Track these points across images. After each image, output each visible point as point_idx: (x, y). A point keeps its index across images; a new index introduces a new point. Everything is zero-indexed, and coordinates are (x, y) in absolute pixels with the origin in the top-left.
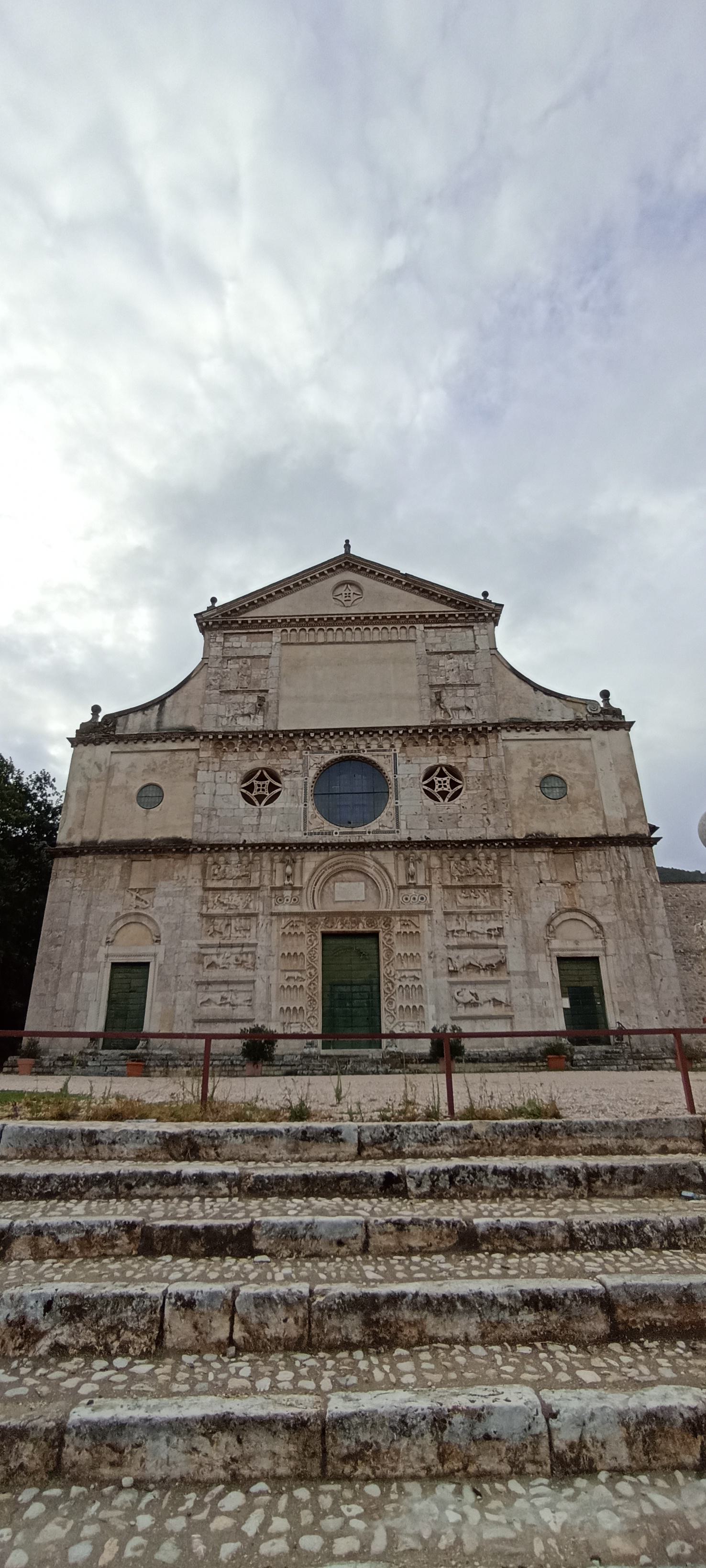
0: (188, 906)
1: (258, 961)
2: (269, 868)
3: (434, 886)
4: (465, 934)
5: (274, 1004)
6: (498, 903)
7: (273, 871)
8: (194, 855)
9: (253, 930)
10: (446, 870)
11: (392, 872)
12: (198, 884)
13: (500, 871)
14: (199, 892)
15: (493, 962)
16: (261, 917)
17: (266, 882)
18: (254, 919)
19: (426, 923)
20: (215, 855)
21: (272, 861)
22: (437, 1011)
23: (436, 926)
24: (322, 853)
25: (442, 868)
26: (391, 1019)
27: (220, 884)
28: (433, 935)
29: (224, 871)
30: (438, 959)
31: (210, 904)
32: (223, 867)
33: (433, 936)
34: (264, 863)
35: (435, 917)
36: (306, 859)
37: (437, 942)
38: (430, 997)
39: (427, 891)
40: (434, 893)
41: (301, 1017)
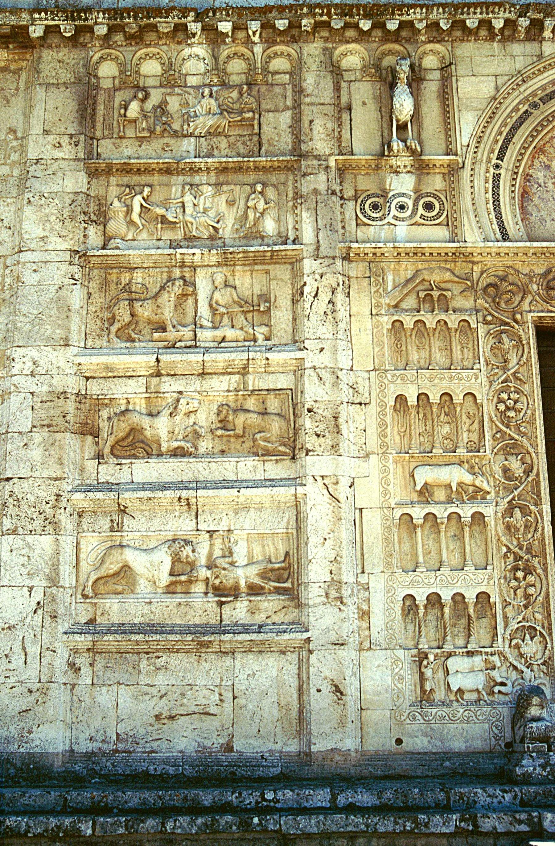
0: (32, 229)
1: (308, 423)
2: (327, 96)
5: (377, 584)
7: (343, 110)
8: (48, 55)
9: (282, 317)
12: (67, 151)
14: (76, 181)
16: (308, 265)
17: (320, 142)
18: (282, 272)
20: (127, 53)
21: (336, 71)
24: (516, 48)
27: (151, 153)
29: (162, 107)
31: (117, 225)
32: (155, 97)
34: (309, 81)
36: (461, 69)
41: (480, 634)
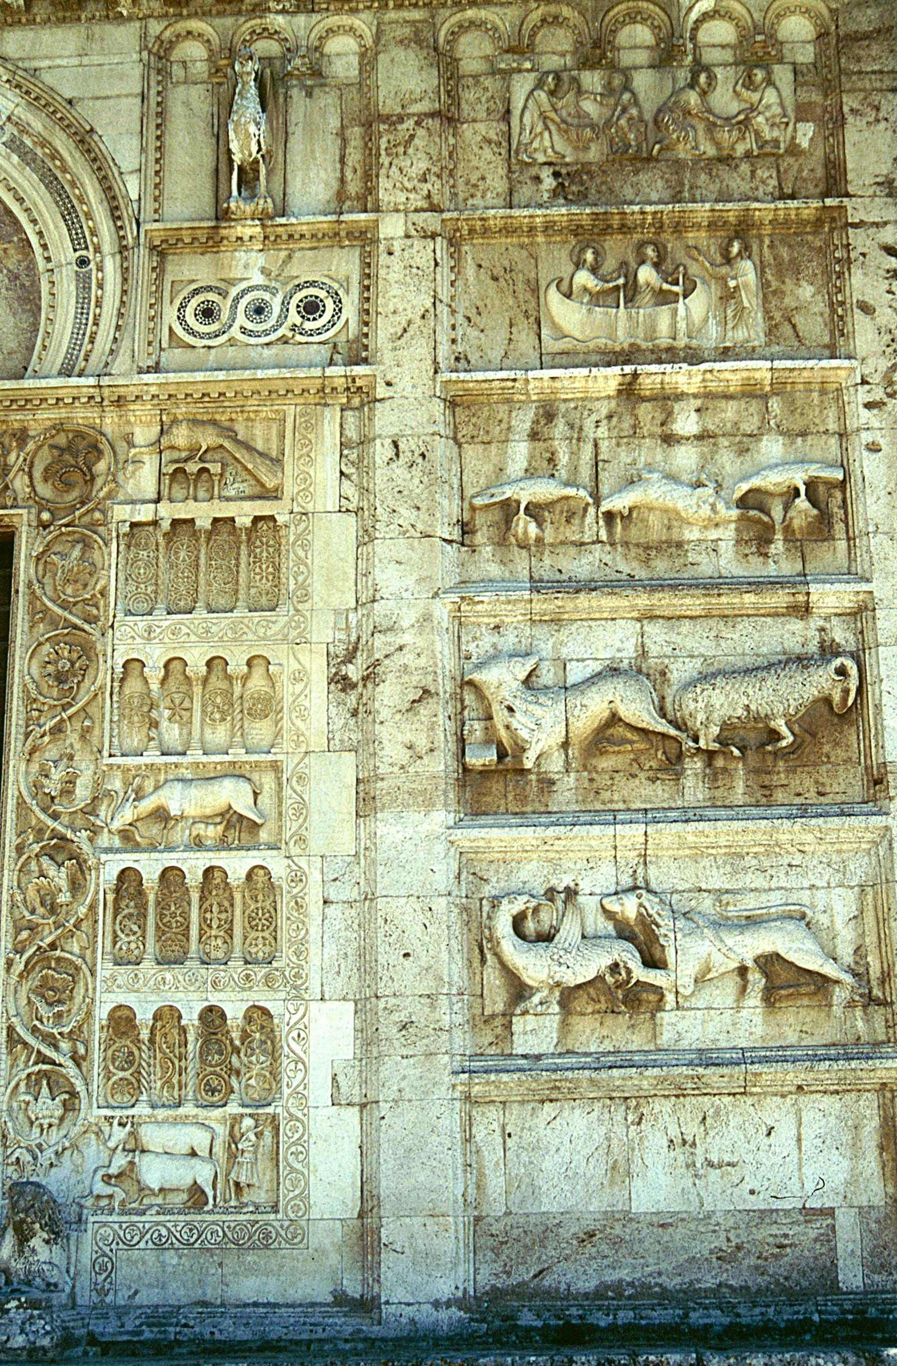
3: (392, 227)
4: (592, 526)
6: (814, 327)
10: (477, 131)
11: (125, 151)
13: (834, 124)
15: (781, 699)
19: (326, 464)
22: (368, 1039)
23: (387, 476)
25: (448, 117)
26: (47, 1107)
28: (366, 537)
30: (389, 695)
33: (364, 553)
35: (385, 421)
37: (389, 579)
38: (320, 942)
39: (345, 264)
40: (391, 271)
